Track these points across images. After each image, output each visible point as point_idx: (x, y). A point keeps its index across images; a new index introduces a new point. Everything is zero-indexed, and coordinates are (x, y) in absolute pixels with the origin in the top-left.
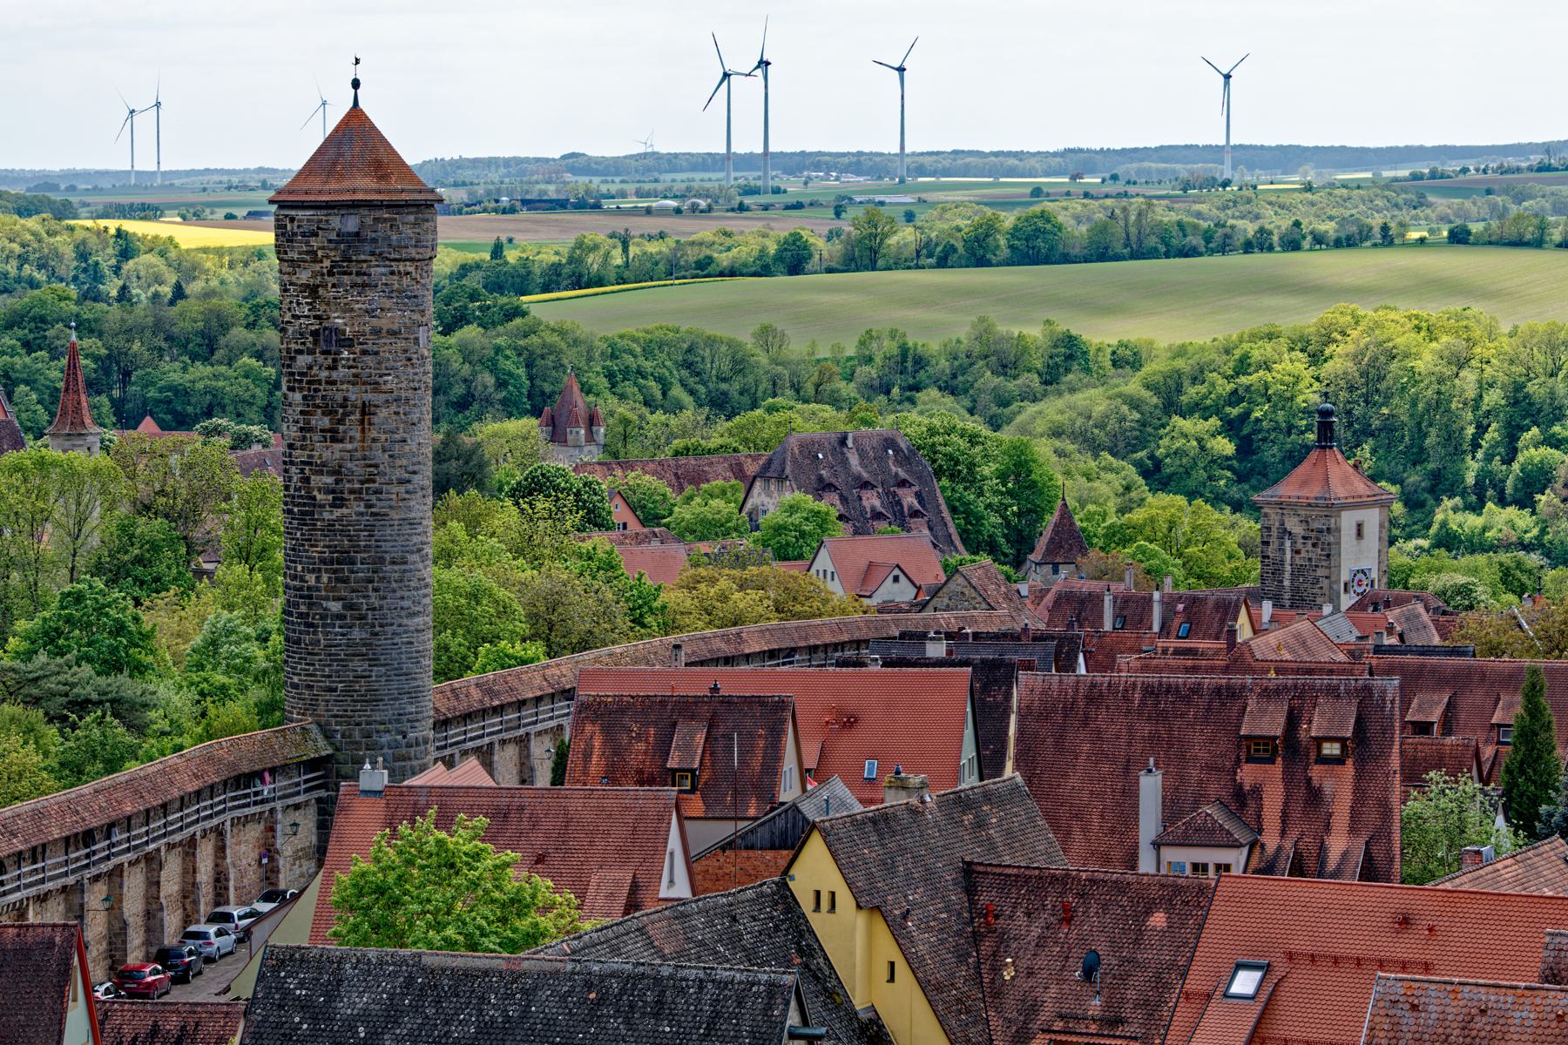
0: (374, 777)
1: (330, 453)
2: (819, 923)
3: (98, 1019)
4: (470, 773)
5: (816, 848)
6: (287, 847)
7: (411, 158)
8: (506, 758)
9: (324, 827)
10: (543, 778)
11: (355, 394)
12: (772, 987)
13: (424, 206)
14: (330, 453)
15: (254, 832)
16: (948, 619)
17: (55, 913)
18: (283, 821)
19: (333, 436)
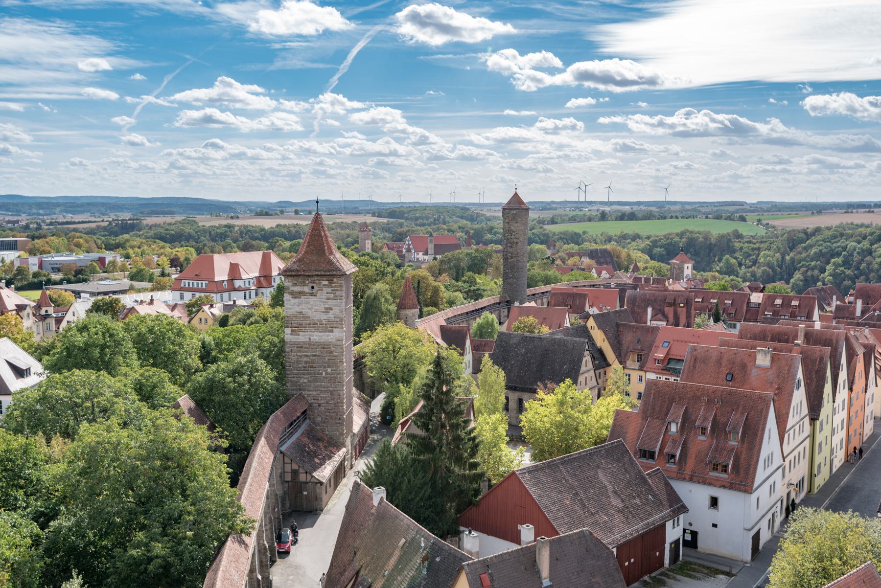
0: (517, 304)
1: (511, 250)
2: (592, 331)
3: (472, 342)
4: (533, 304)
5: (591, 319)
6: (502, 315)
7: (525, 201)
8: (539, 301)
9: (509, 312)
10: (545, 306)
11: (515, 240)
12: (584, 342)
13: (527, 209)
14: (511, 250)
15: (497, 312)
16: (616, 281)
17: (465, 325)
18: (502, 311)
19: (511, 247)
